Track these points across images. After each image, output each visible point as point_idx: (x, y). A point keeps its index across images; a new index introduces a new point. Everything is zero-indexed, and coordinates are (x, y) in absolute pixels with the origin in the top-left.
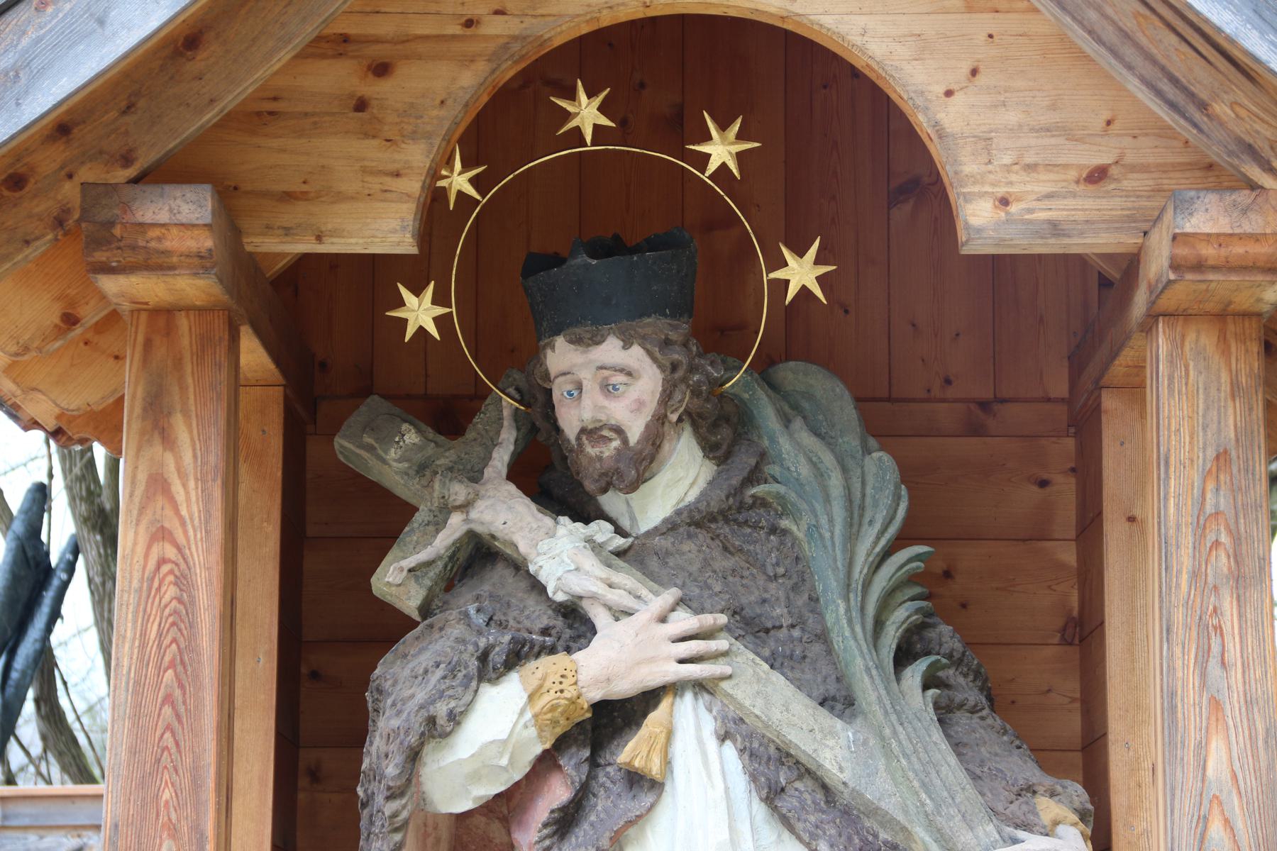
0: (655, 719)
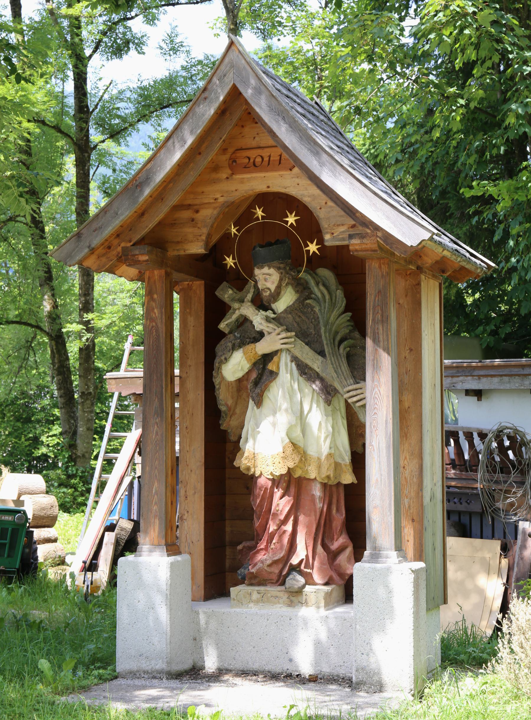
0: (275, 359)
